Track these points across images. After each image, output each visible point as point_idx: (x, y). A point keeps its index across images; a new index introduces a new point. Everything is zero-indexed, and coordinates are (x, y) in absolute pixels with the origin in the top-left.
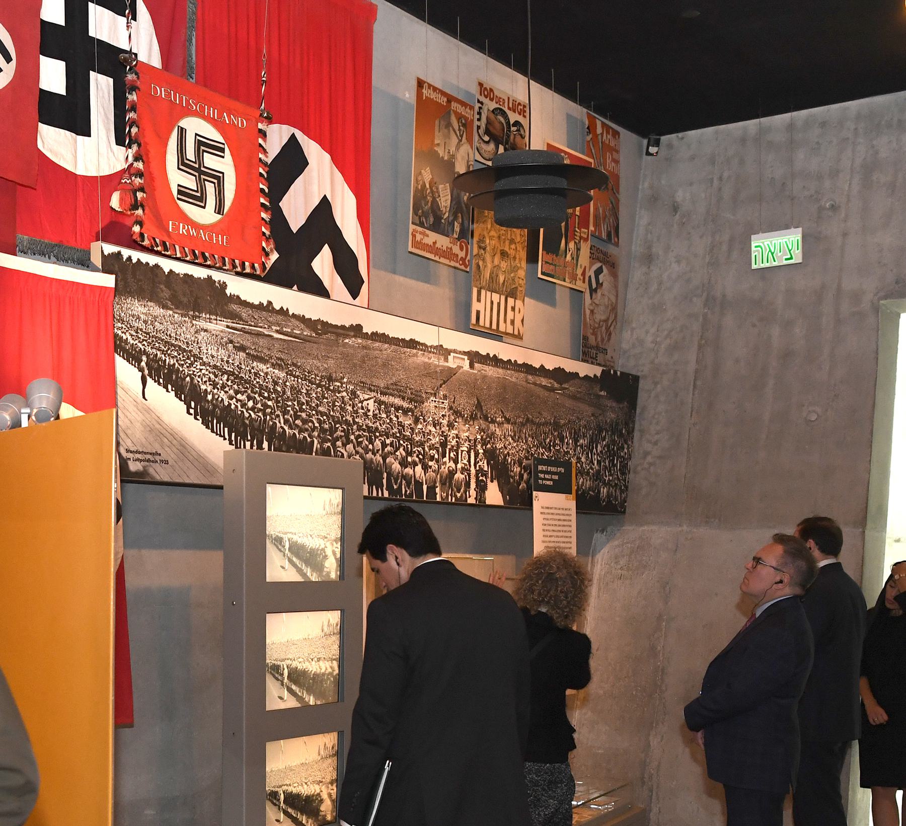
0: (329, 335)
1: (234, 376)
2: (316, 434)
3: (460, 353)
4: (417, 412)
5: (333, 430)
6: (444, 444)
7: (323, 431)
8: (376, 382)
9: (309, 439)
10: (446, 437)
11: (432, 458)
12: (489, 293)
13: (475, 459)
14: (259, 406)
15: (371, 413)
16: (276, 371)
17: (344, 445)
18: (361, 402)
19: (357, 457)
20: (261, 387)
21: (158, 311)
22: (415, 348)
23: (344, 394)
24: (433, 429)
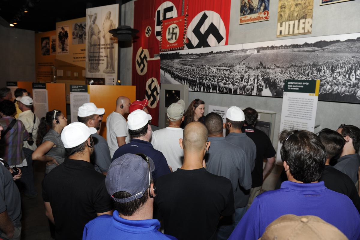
0: (203, 56)
1: (180, 69)
2: (198, 78)
3: (253, 49)
4: (231, 70)
5: (202, 77)
6: (242, 78)
7: (200, 78)
8: (216, 64)
9: (196, 80)
10: (243, 76)
11: (236, 82)
12: (287, 23)
13: (257, 81)
14: (185, 74)
15: (214, 72)
16: (189, 67)
17: (205, 80)
18: (211, 70)
19: (209, 83)
20: (185, 70)
21: (167, 61)
22: (232, 52)
23: (206, 69)
24: (238, 74)
